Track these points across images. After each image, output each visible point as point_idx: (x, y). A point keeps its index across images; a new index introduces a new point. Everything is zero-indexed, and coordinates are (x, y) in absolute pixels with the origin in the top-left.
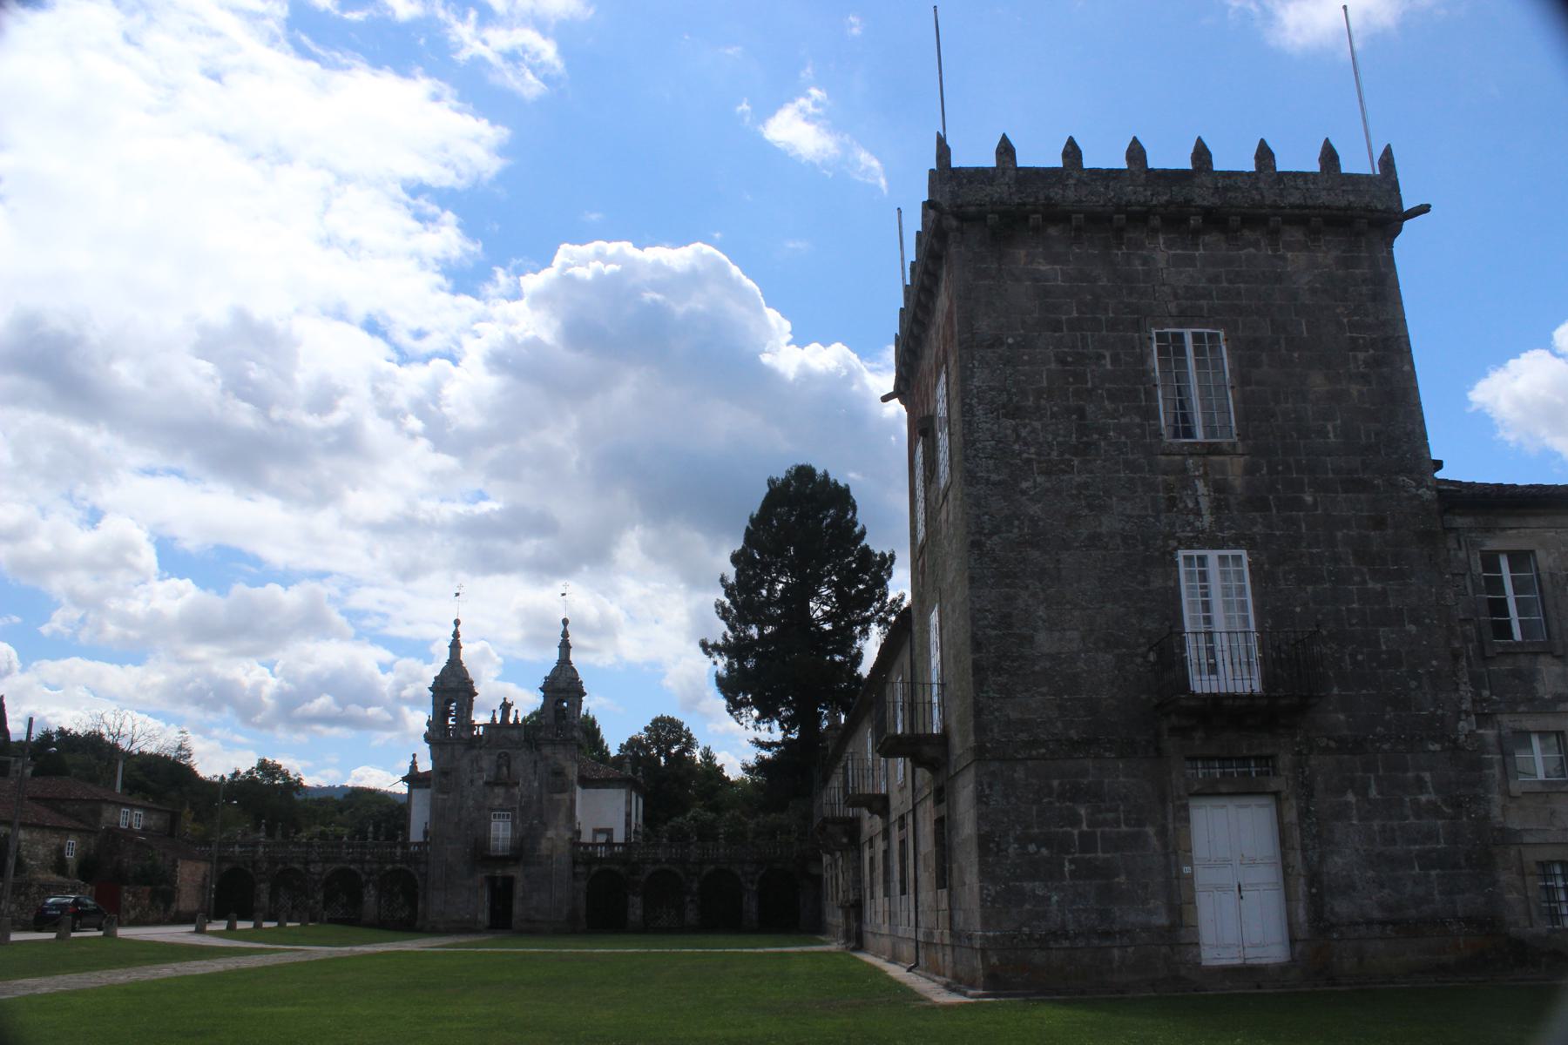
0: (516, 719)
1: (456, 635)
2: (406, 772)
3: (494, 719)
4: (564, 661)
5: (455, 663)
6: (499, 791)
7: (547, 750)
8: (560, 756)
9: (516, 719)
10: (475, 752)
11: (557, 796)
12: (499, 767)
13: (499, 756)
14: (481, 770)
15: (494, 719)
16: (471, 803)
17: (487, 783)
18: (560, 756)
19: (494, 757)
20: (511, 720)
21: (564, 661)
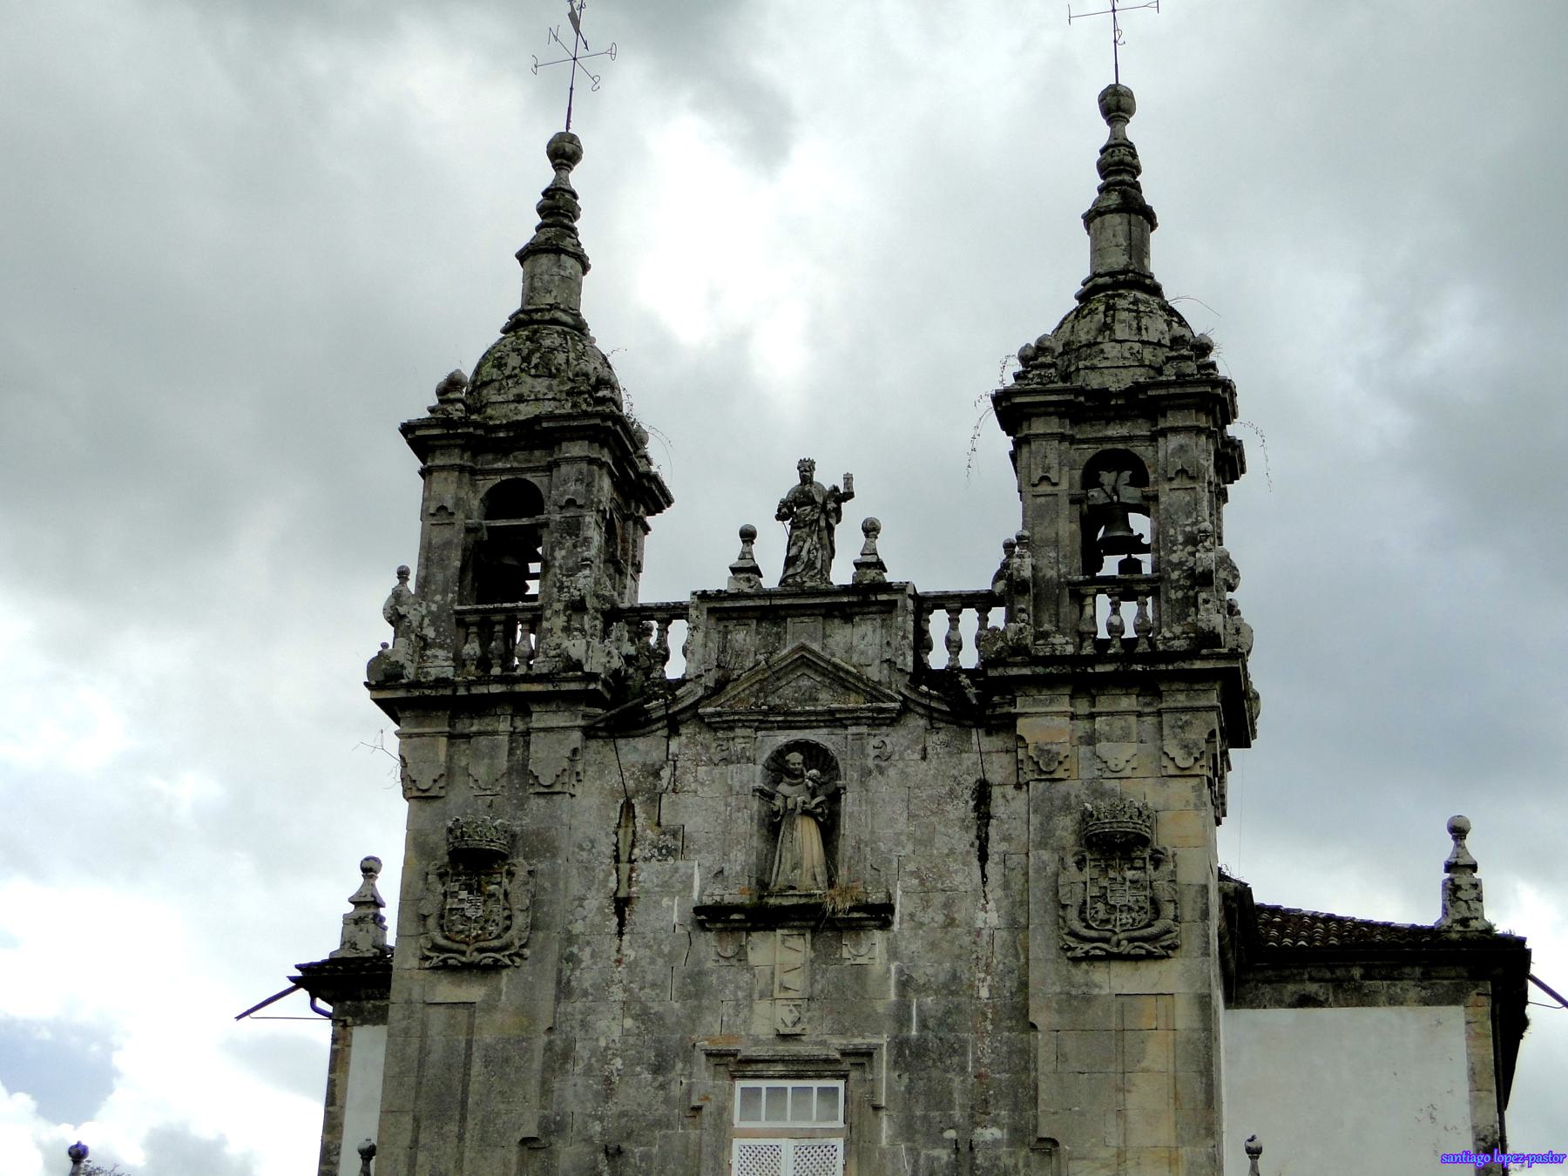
0: (870, 564)
1: (558, 209)
2: (324, 945)
3: (747, 570)
4: (1120, 284)
5: (546, 324)
6: (779, 955)
7: (1046, 723)
8: (1119, 754)
9: (870, 564)
10: (640, 750)
11: (1114, 980)
12: (773, 826)
13: (778, 767)
14: (674, 845)
15: (747, 570)
16: (612, 1027)
17: (711, 917)
18: (1119, 754)
19: (755, 775)
20: (842, 573)
21: (1120, 284)
